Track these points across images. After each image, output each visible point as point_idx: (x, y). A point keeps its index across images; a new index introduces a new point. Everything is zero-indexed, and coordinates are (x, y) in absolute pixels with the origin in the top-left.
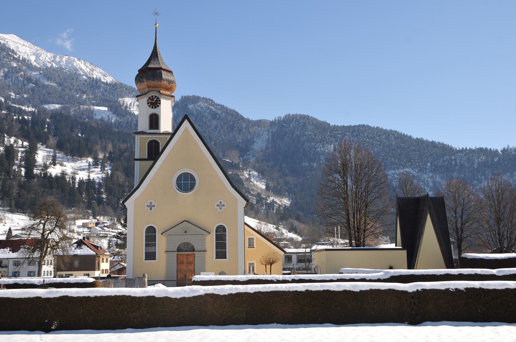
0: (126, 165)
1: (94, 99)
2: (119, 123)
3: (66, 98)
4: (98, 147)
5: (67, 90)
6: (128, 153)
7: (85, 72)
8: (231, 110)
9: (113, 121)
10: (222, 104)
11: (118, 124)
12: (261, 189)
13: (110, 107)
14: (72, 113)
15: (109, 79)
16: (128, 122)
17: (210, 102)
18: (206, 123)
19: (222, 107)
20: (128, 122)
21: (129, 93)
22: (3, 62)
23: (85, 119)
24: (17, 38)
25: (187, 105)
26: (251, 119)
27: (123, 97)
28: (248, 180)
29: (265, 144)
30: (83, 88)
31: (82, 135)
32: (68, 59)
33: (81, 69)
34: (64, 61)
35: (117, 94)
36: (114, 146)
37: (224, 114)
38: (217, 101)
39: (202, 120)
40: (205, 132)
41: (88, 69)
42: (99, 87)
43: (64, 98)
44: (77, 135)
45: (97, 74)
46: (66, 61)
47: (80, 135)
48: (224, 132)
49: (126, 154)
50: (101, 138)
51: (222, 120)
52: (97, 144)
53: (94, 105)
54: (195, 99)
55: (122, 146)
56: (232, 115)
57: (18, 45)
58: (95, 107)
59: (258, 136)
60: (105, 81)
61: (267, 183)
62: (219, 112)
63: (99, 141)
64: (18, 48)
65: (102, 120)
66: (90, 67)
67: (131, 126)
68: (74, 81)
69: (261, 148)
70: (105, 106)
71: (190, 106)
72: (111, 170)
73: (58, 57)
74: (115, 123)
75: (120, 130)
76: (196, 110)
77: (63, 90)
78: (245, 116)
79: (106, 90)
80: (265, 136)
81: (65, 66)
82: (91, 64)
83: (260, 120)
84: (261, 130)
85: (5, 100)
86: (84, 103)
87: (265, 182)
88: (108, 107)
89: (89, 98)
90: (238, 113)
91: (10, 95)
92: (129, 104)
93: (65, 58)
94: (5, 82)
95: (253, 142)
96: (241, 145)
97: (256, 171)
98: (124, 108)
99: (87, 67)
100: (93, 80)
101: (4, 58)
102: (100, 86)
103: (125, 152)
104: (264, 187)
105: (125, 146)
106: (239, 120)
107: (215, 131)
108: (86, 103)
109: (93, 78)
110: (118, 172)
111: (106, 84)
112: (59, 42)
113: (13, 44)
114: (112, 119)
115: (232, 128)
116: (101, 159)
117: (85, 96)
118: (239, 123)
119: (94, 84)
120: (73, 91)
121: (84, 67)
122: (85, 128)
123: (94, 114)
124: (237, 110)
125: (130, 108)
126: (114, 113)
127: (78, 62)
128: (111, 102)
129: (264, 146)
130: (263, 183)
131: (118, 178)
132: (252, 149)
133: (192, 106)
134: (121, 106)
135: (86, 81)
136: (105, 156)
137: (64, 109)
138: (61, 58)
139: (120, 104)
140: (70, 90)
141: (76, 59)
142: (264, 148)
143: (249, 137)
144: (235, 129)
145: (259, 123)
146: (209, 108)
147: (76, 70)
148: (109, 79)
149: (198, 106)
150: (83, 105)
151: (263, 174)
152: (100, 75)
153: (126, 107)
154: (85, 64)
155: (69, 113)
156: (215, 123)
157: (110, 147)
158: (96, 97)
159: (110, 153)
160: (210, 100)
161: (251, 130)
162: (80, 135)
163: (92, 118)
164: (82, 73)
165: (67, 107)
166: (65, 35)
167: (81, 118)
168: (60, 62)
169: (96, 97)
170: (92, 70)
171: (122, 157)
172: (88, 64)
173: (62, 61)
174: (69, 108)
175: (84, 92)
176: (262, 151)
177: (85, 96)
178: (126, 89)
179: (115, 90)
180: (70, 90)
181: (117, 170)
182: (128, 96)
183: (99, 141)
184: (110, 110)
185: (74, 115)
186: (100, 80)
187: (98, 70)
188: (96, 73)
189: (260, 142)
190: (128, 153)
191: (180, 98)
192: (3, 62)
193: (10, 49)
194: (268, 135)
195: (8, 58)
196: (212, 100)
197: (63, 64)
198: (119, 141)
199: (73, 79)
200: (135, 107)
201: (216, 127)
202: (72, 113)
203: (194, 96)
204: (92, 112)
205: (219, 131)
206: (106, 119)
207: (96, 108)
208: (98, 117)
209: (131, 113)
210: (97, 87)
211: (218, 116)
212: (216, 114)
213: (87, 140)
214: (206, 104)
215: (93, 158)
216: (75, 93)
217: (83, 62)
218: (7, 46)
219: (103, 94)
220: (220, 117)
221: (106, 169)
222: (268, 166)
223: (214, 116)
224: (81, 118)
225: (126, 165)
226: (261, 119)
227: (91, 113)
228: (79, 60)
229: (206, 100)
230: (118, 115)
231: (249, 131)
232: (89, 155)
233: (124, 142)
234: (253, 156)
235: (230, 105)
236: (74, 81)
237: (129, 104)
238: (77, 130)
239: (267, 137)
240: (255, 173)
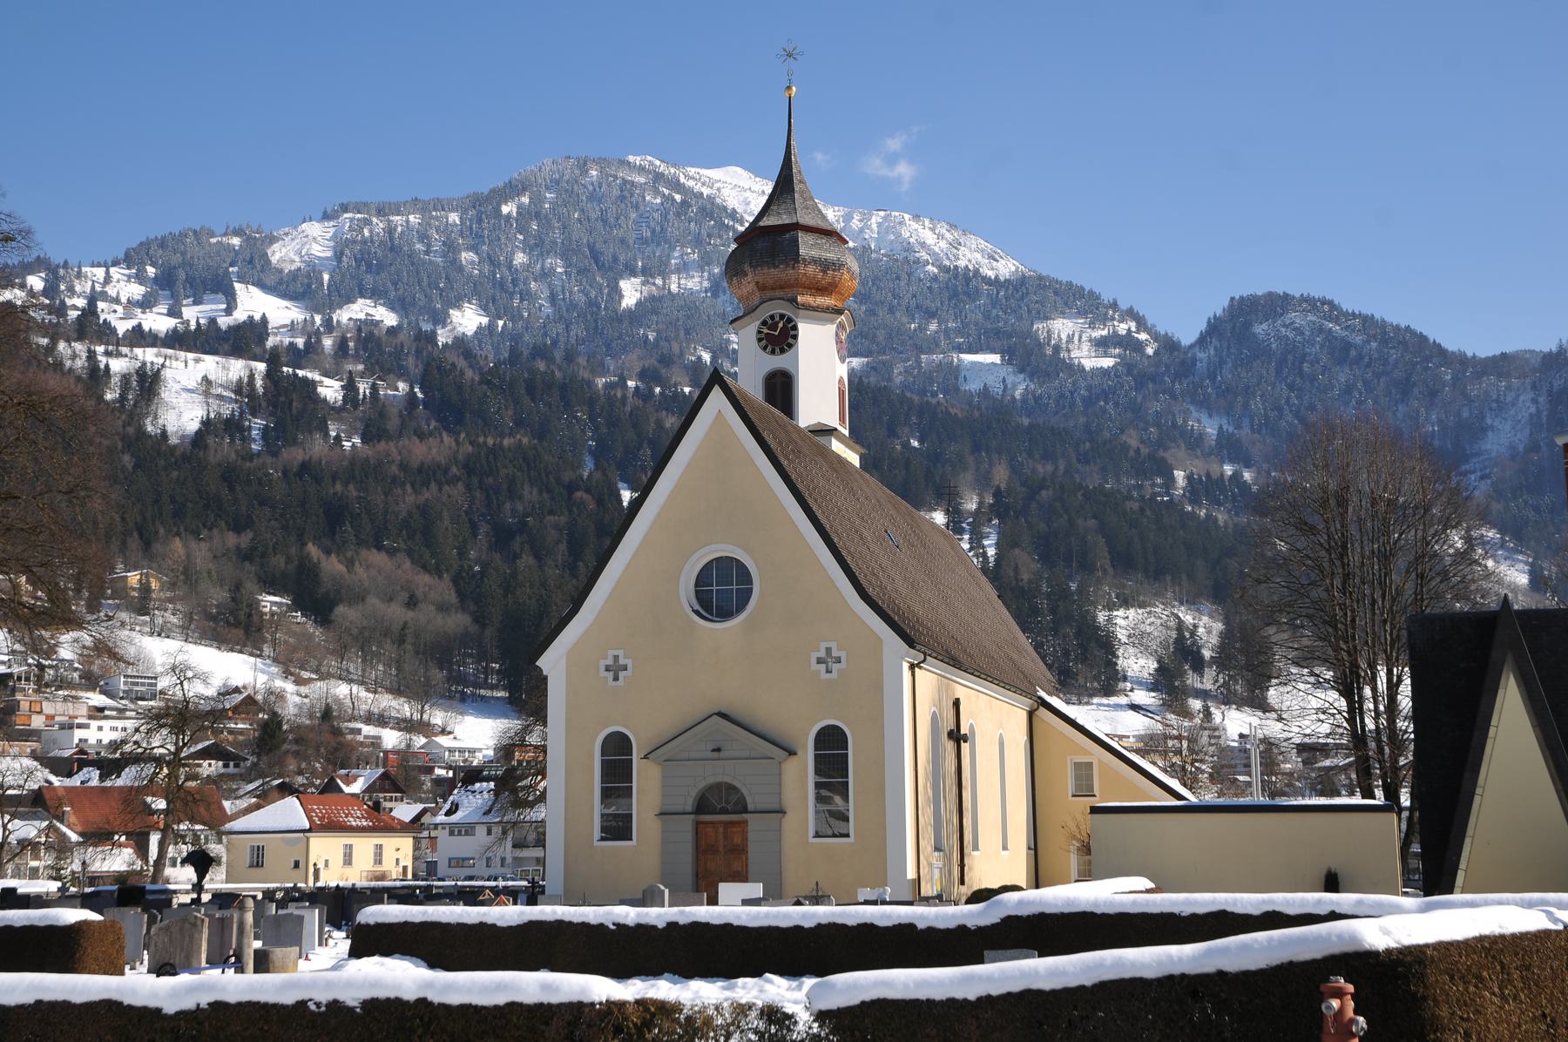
0: (1042, 527)
1: (959, 332)
2: (1037, 399)
3: (881, 335)
4: (969, 476)
5: (882, 312)
6: (1051, 492)
7: (935, 254)
8: (1397, 328)
9: (1018, 394)
10: (1366, 311)
11: (1032, 404)
12: (1515, 588)
13: (1009, 354)
14: (898, 380)
15: (1006, 266)
16: (1062, 396)
17: (1325, 308)
18: (1313, 379)
19: (1367, 321)
20: (1062, 396)
21: (1066, 304)
22: (709, 248)
23: (934, 395)
24: (745, 174)
25: (1247, 325)
26: (1470, 354)
27: (1047, 318)
28: (1464, 557)
29: (1527, 431)
30: (928, 303)
31: (921, 441)
32: (885, 218)
33: (923, 245)
34: (874, 226)
35: (1029, 311)
36: (1015, 470)
37: (1374, 345)
38: (1348, 305)
39: (1301, 369)
40: (1312, 408)
41: (943, 244)
42: (973, 295)
43: (875, 336)
44: (907, 445)
45: (972, 254)
46: (879, 225)
47: (916, 444)
48: (1375, 402)
49: (1044, 493)
50: (976, 449)
51: (1369, 365)
52: (965, 469)
53: (960, 349)
54: (1275, 305)
55: (1040, 469)
56: (1403, 343)
57: (748, 194)
58: (963, 356)
59: (1501, 407)
60: (991, 274)
61: (1532, 565)
62: (1358, 339)
63: (970, 460)
64: (748, 204)
65: (985, 392)
66: (948, 235)
67: (1073, 405)
68: (903, 284)
69: (1512, 447)
70: (993, 351)
71: (1260, 329)
72: (998, 545)
73: (857, 217)
74: (1024, 400)
75: (1040, 421)
76: (1279, 338)
77: (872, 312)
78: (1450, 345)
79: (994, 302)
80: (1526, 405)
81: (877, 240)
82: (953, 226)
83: (1504, 355)
84: (1508, 388)
85: (714, 359)
86: (932, 345)
87: (1526, 563)
88: (1002, 352)
89: (947, 331)
90: (1422, 338)
91: (728, 341)
92: (1064, 337)
93: (875, 220)
94: (713, 306)
95: (1477, 429)
96: (1436, 443)
97: (1493, 526)
98: (1049, 351)
99: (940, 236)
100: (956, 276)
101: (709, 236)
102: (977, 290)
103: (1042, 487)
104: (1523, 580)
105: (1050, 468)
106: (1428, 359)
107: (1346, 404)
108: (937, 345)
109: (956, 267)
110: (1017, 551)
111: (995, 282)
112: (874, 166)
113: (734, 193)
114: (1014, 387)
115: (1404, 388)
116: (971, 514)
117: (933, 327)
118: (1427, 368)
119: (961, 286)
120: (898, 314)
121: (929, 238)
122: (932, 422)
123: (961, 379)
124: (1419, 327)
125: (1069, 351)
126: (1022, 371)
127: (914, 225)
128: (1010, 336)
129: (1521, 438)
130: (1521, 566)
131: (1016, 569)
132: (1477, 455)
133: (1264, 326)
134: (1040, 346)
135: (935, 278)
136: (981, 504)
137: (874, 368)
138: (865, 219)
139: (1037, 339)
140: (891, 311)
141: (907, 216)
142: (1521, 448)
143: (1465, 414)
144: (1416, 390)
145: (1501, 364)
146: (1321, 330)
147: (909, 248)
148: (1006, 268)
149: (1285, 326)
150: (930, 352)
151: (1518, 535)
152: (978, 256)
153: (1057, 348)
154: (933, 230)
155: (890, 379)
156: (1343, 376)
157: (1001, 475)
158: (968, 325)
159: (997, 494)
160: (1324, 302)
161: (1474, 390)
162: (916, 444)
163: (957, 390)
164: (923, 255)
165: (884, 363)
166: (894, 144)
167: (923, 392)
168: (861, 230)
169: (965, 325)
170: (956, 245)
171: (1034, 505)
172: (942, 228)
173: (869, 227)
174: (888, 366)
175: (931, 315)
176: (1513, 458)
177: (933, 327)
178: (1056, 293)
179: (1022, 298)
180: (891, 311)
181: (1015, 544)
182: (1063, 314)
183: (970, 460)
184: (1010, 362)
185: (905, 386)
186: (977, 272)
187: (974, 241)
188: (967, 251)
189: (1508, 427)
190: (1051, 492)
191: (1226, 303)
192: (709, 248)
193: (725, 208)
194: (1534, 401)
195: (720, 237)
196: (1330, 303)
197: (872, 234)
198: (1030, 454)
199: (898, 278)
200: (1086, 346)
201: (1348, 390)
202: (898, 380)
203: (1270, 294)
204: (955, 371)
205: (1360, 403)
206: (997, 389)
207: (968, 358)
208: (974, 386)
209: (1071, 366)
210: (969, 295)
211: (1353, 353)
212: (1347, 346)
213: (935, 457)
214: (1311, 317)
215: (947, 512)
216: (905, 319)
217: (927, 222)
218: (718, 201)
219: (987, 316)
220: (1360, 357)
221: (986, 543)
222: (1537, 509)
223: (1341, 352)
224: (923, 392)
225: (1042, 527)
226: (1509, 348)
227: (953, 373)
228: (916, 217)
229: (1311, 304)
230: (1031, 377)
231: (1464, 394)
232: (938, 504)
233: (1048, 456)
234: (1482, 478)
235: (1395, 313)
236: (903, 284)
237: (1064, 337)
238: (906, 430)
239: (1533, 410)
240: (1491, 534)
